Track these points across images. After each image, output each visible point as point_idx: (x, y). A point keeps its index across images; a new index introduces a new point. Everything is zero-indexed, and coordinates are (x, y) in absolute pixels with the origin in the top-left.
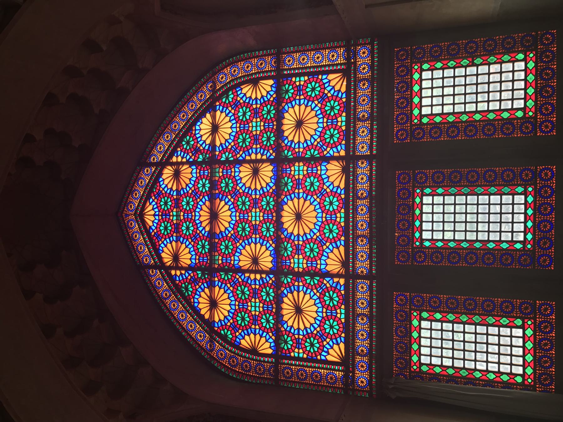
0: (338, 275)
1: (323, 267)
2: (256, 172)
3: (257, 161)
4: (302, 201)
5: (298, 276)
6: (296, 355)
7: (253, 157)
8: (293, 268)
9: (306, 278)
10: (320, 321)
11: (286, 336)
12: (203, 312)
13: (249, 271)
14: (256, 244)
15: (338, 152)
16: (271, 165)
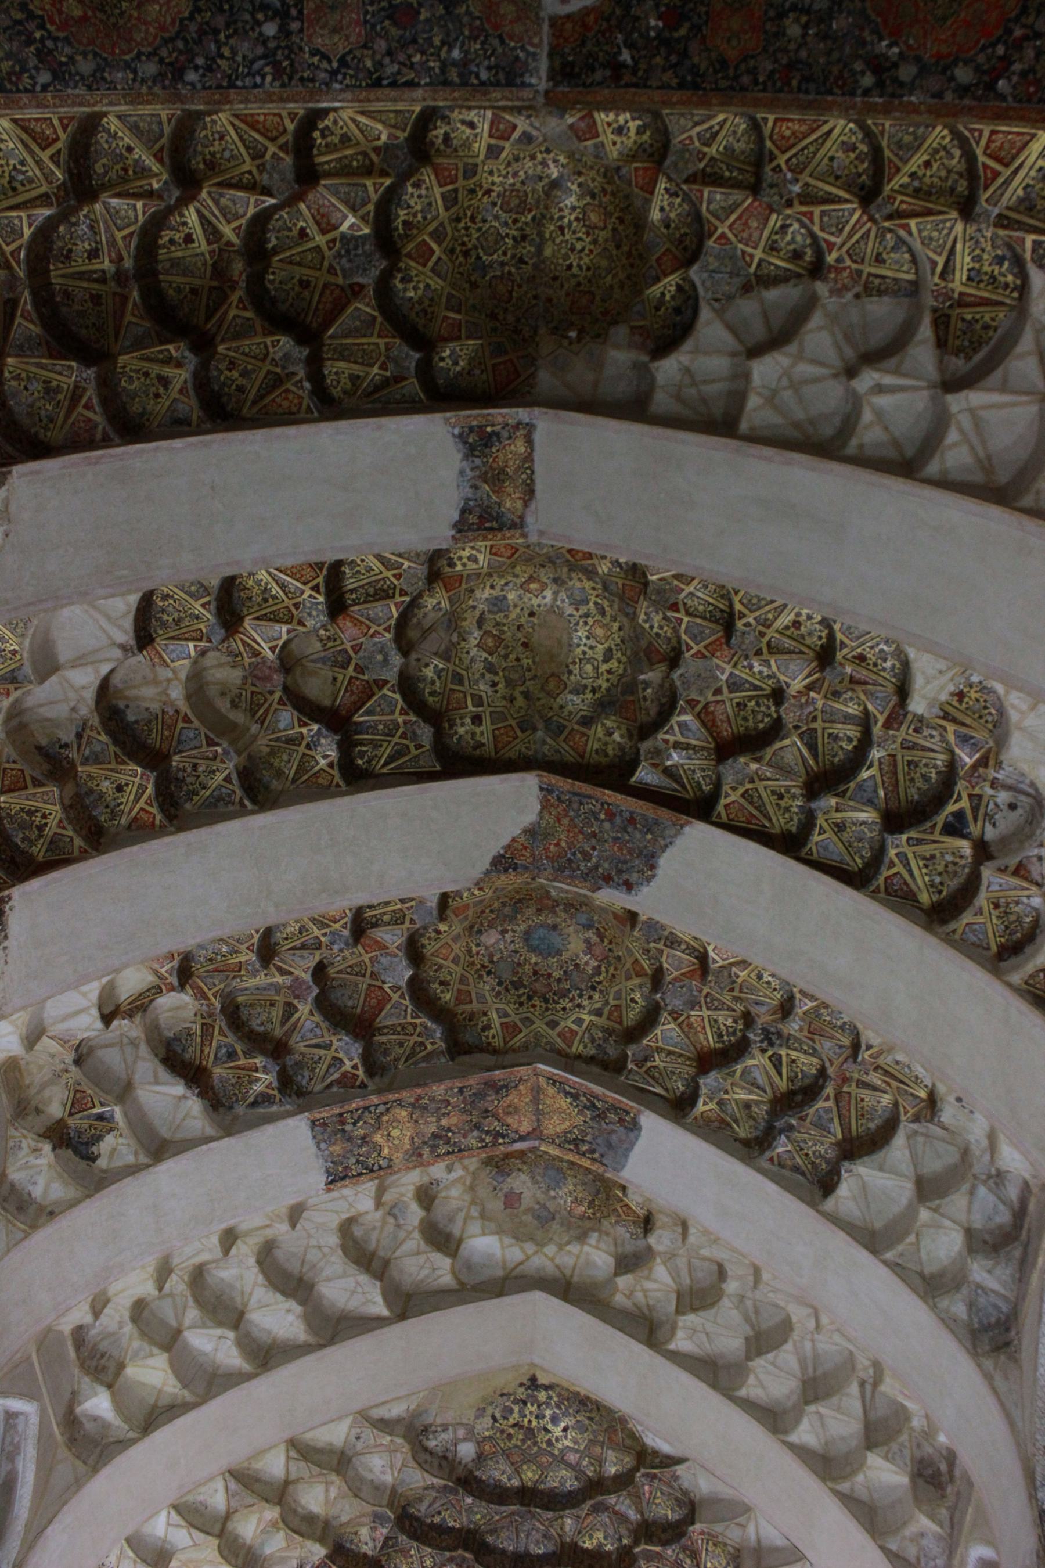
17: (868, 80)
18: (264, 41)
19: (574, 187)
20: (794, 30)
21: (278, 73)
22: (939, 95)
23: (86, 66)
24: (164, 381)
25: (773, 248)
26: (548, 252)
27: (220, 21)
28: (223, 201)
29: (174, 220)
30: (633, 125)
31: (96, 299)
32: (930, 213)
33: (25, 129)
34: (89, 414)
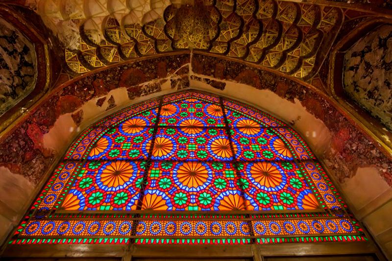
0: (140, 203)
1: (150, 192)
2: (223, 148)
3: (232, 148)
4: (206, 176)
5: (145, 176)
6: (83, 172)
7: (235, 146)
8: (151, 170)
9: (142, 179)
10: (104, 190)
11: (99, 164)
12: (131, 121)
13: (153, 142)
14: (173, 147)
15: (251, 204)
16: (231, 157)
17: (140, 63)
18: (230, 67)
19: (188, 33)
20: (153, 67)
21: (229, 63)
22: (128, 64)
23: (256, 71)
24: (264, 10)
25: (152, 29)
26: (193, 21)
27: (235, 71)
28: (243, 42)
29: (253, 39)
30: (178, 45)
31: (272, 28)
32: (126, 44)
33: (269, 64)
34: (281, 8)
